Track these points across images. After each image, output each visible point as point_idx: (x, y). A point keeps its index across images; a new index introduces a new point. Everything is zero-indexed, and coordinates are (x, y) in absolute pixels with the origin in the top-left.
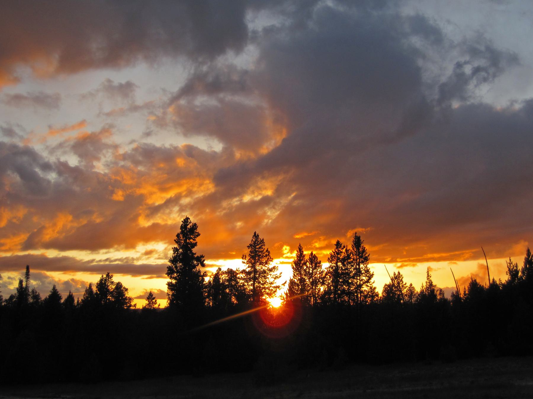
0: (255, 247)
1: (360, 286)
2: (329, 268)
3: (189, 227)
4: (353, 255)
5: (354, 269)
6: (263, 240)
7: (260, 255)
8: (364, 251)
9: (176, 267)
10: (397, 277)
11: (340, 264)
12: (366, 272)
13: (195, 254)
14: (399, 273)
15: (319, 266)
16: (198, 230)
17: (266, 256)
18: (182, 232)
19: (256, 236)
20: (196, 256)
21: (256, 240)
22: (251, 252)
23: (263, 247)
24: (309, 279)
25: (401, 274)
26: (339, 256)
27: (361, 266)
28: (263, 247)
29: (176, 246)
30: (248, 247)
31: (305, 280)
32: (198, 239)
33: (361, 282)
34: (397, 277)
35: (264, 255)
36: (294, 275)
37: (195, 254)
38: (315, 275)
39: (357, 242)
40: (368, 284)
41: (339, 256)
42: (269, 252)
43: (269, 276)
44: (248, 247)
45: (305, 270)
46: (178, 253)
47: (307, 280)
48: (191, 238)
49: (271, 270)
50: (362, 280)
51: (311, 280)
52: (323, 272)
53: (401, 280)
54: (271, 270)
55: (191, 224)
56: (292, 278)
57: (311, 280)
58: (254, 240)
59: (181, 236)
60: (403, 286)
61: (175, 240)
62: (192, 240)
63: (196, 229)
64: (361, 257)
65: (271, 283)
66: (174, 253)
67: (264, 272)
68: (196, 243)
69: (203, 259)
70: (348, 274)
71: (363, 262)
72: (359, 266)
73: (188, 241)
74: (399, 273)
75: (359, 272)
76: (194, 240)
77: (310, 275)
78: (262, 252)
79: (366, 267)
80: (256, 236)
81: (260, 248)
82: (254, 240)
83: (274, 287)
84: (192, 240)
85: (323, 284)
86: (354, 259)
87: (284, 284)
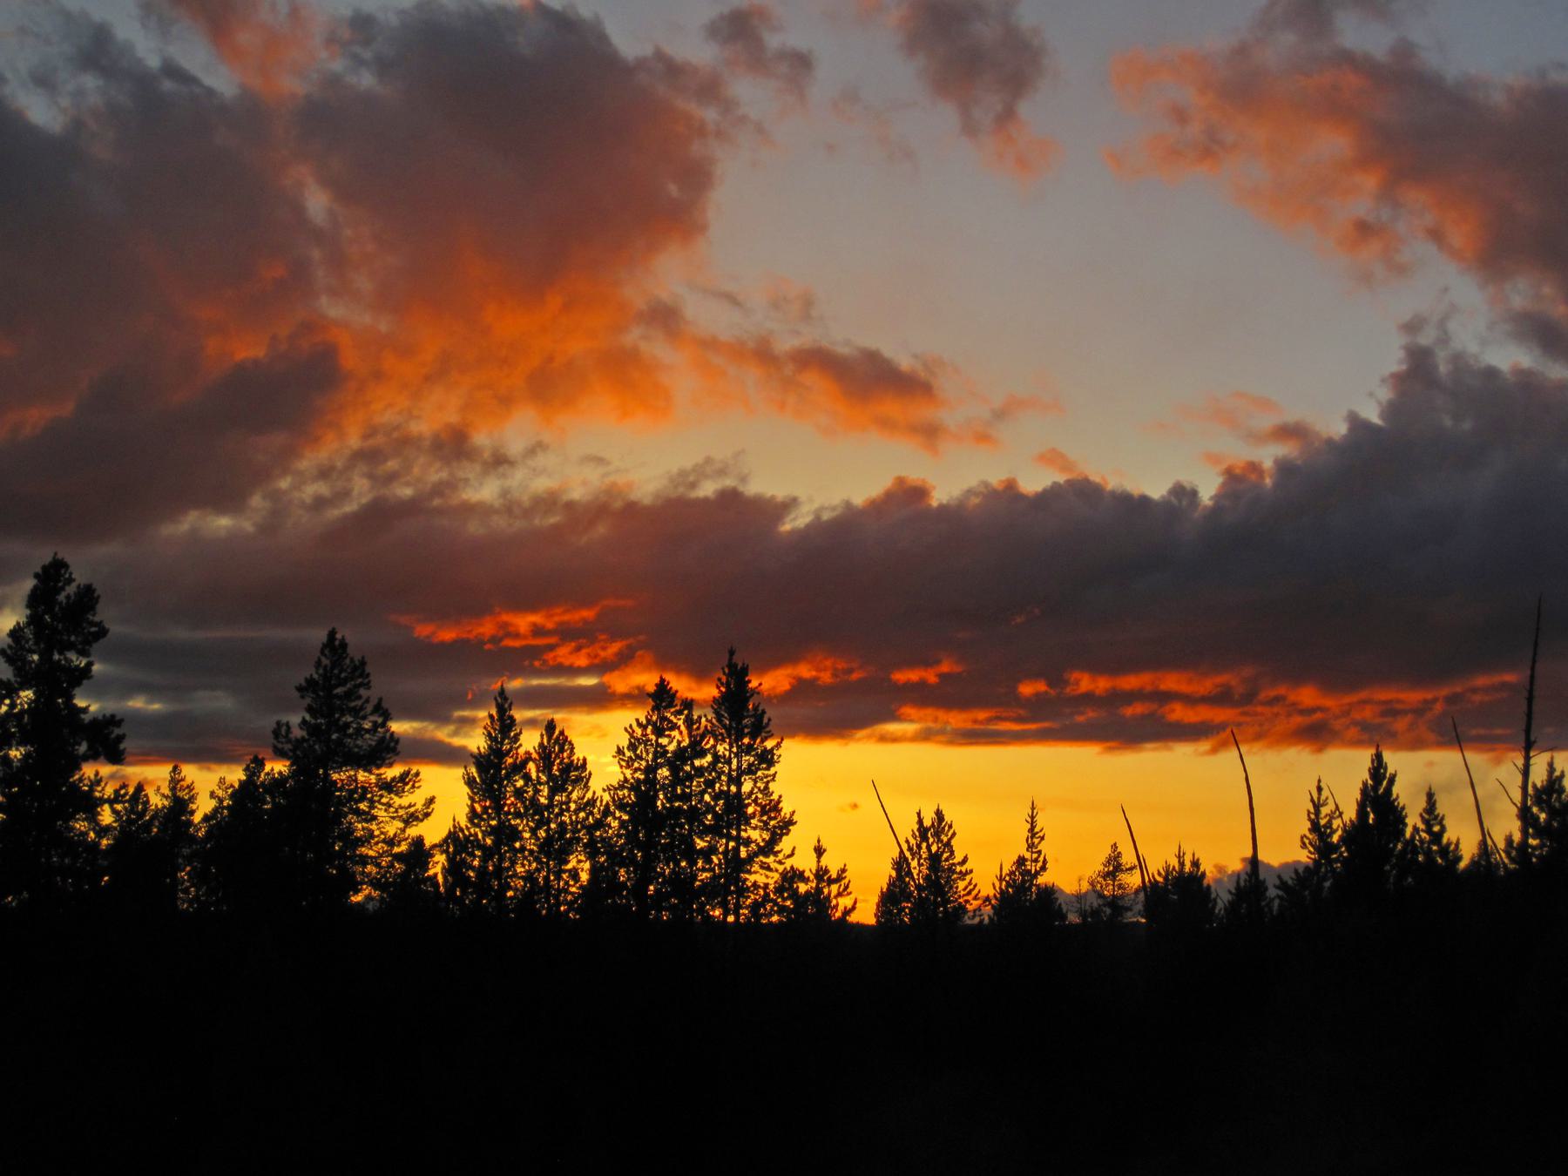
1: (737, 866)
2: (621, 787)
3: (62, 597)
5: (716, 797)
6: (363, 663)
7: (347, 725)
10: (934, 831)
11: (664, 772)
12: (764, 812)
14: (939, 815)
15: (579, 779)
16: (105, 614)
19: (334, 647)
21: (334, 665)
22: (309, 709)
23: (362, 691)
24: (534, 831)
25: (948, 819)
26: (663, 741)
28: (362, 691)
30: (300, 689)
31: (515, 834)
33: (743, 853)
34: (934, 831)
35: (367, 725)
36: (473, 809)
38: (561, 813)
40: (770, 860)
41: (663, 741)
43: (380, 812)
45: (519, 793)
46: (12, 706)
47: (527, 835)
48: (71, 646)
49: (389, 787)
51: (542, 833)
52: (592, 802)
53: (948, 844)
54: (389, 787)
55: (71, 589)
56: (464, 822)
57: (542, 833)
60: (951, 870)
64: (749, 749)
65: (391, 842)
69: (117, 731)
70: (694, 815)
71: (751, 770)
72: (739, 785)
73: (56, 657)
74: (939, 815)
75: (735, 809)
76: (83, 653)
79: (766, 791)
80: (334, 647)
81: (349, 695)
82: (325, 661)
84: (72, 656)
86: (716, 758)
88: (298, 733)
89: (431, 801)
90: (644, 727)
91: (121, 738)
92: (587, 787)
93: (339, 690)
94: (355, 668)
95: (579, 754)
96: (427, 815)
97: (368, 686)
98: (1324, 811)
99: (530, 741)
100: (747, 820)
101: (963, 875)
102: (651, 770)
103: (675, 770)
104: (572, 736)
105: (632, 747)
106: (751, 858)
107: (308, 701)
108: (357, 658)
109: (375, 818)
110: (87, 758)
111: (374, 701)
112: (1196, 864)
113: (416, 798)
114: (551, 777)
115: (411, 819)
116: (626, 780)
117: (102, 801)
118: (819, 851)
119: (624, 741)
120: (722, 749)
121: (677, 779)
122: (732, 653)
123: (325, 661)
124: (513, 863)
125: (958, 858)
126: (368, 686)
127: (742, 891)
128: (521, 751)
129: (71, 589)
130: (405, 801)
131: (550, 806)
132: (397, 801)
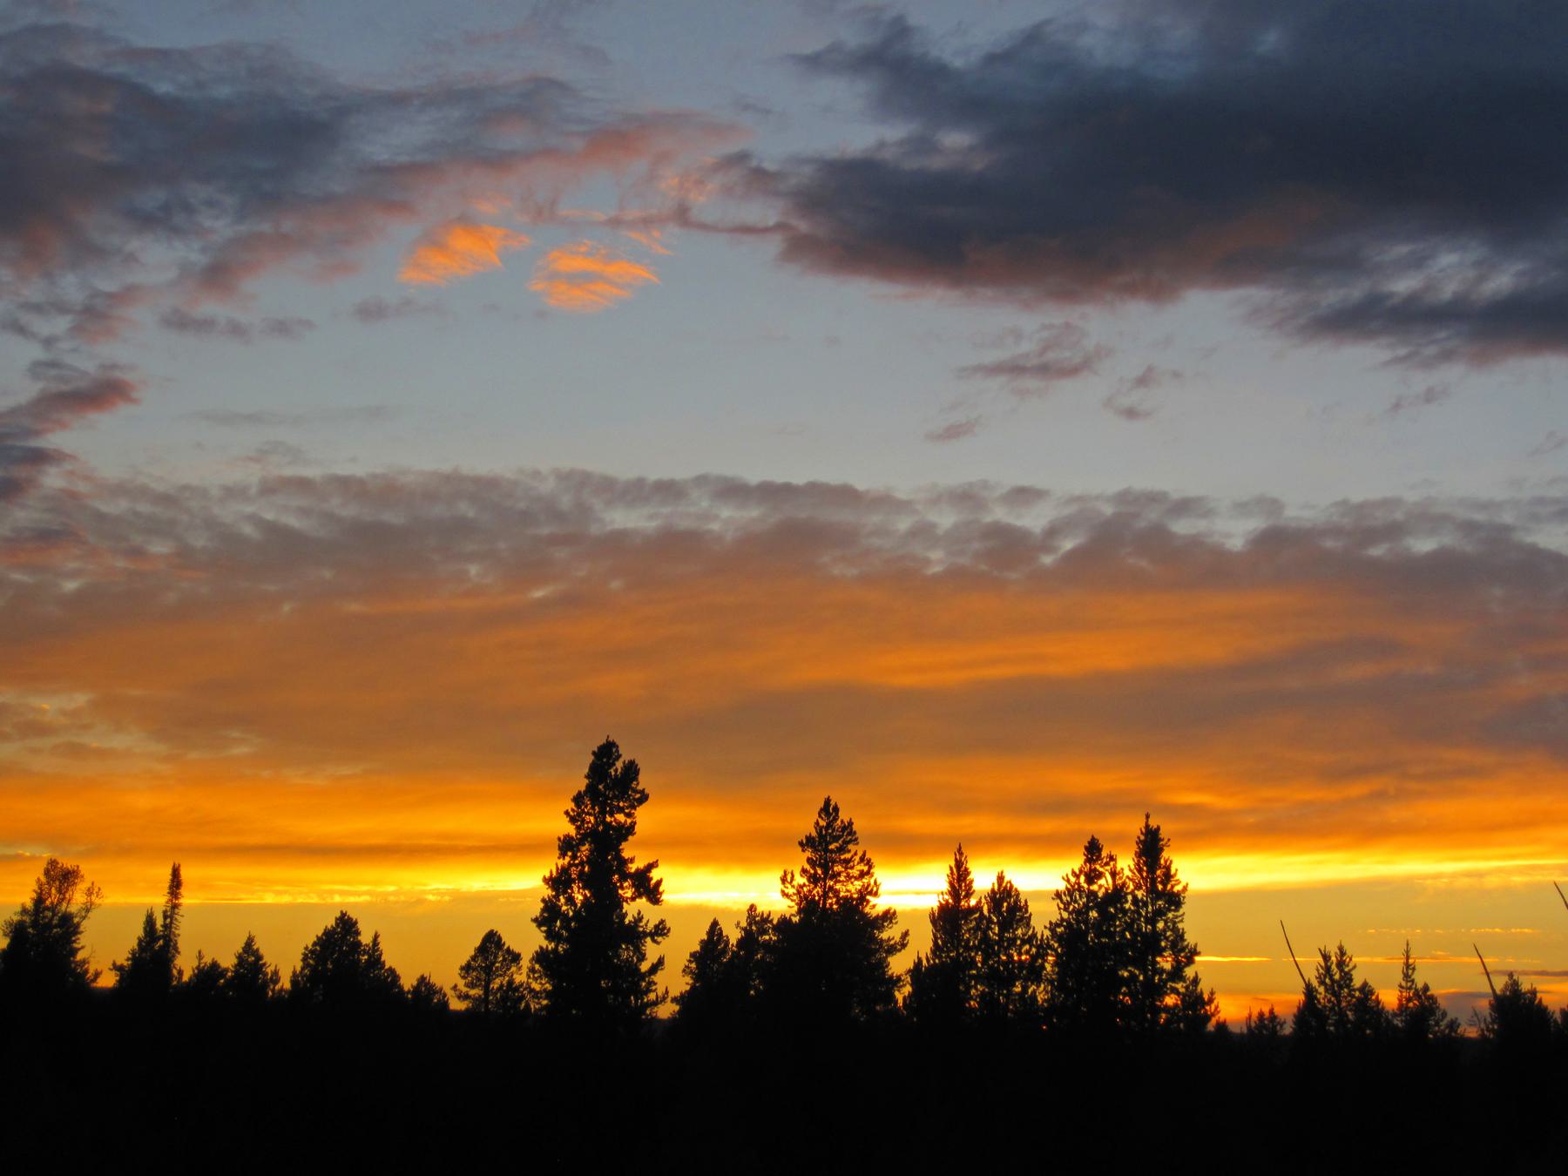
6: (851, 823)
8: (1168, 876)
11: (1094, 914)
14: (1341, 948)
16: (644, 782)
17: (862, 875)
18: (591, 790)
19: (829, 810)
20: (633, 868)
21: (829, 825)
22: (809, 860)
24: (983, 963)
26: (1095, 887)
27: (1161, 925)
28: (850, 847)
29: (571, 830)
30: (801, 844)
35: (855, 872)
36: (935, 942)
37: (632, 860)
38: (1009, 947)
39: (1151, 848)
40: (1180, 986)
41: (1095, 887)
42: (869, 864)
46: (574, 857)
48: (621, 810)
50: (1163, 971)
55: (619, 765)
58: (823, 823)
61: (567, 813)
62: (621, 817)
63: (635, 778)
66: (563, 855)
68: (633, 825)
71: (1159, 913)
72: (1154, 927)
73: (608, 819)
76: (629, 815)
77: (987, 946)
78: (847, 861)
80: (829, 810)
82: (823, 823)
84: (621, 817)
89: (906, 934)
90: (1078, 877)
91: (659, 883)
92: (1028, 925)
93: (832, 847)
94: (844, 828)
96: (904, 946)
97: (855, 841)
102: (1081, 913)
107: (808, 854)
108: (846, 821)
110: (633, 899)
111: (860, 854)
116: (1062, 920)
117: (645, 934)
121: (1105, 917)
122: (1148, 817)
124: (968, 988)
126: (855, 841)
127: (1156, 1011)
129: (619, 765)
131: (998, 943)
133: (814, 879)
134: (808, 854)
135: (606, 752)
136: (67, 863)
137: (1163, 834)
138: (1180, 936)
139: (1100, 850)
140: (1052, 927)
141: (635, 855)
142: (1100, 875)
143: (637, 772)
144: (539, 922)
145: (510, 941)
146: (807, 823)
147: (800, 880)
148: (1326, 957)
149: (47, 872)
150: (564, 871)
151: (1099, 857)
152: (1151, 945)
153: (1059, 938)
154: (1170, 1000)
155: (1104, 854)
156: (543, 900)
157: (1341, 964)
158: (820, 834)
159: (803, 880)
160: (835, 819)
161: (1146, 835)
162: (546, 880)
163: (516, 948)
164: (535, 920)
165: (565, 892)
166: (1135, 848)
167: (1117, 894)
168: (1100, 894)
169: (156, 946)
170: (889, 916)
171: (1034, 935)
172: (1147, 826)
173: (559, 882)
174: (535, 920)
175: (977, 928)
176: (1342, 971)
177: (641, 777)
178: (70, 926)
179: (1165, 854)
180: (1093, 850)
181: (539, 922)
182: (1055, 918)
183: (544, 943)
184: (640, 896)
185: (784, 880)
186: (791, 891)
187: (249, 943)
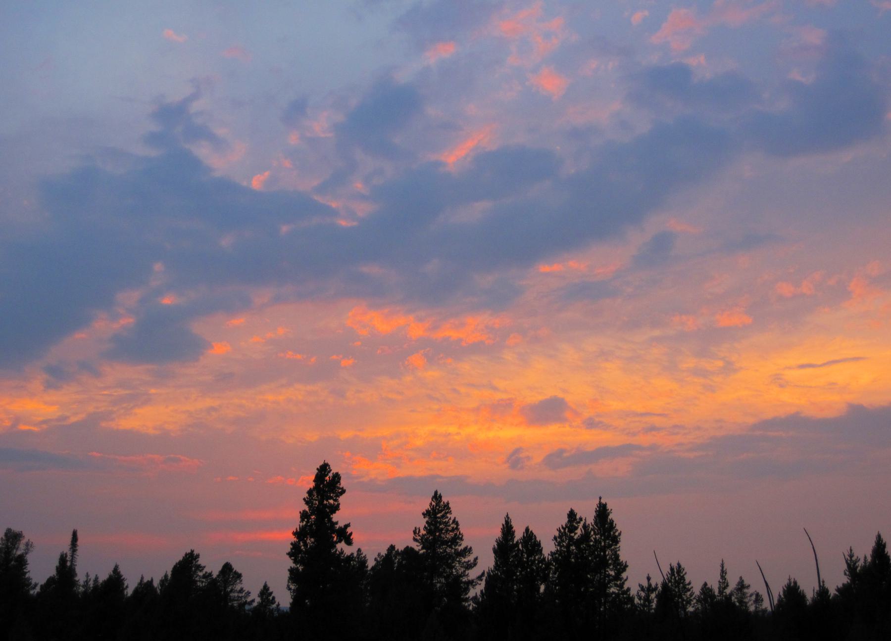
0: (435, 513)
1: (605, 586)
3: (327, 478)
4: (595, 534)
6: (448, 503)
7: (442, 529)
9: (305, 544)
13: (337, 523)
16: (343, 483)
18: (317, 488)
19: (437, 497)
20: (337, 526)
22: (427, 522)
23: (448, 515)
28: (448, 515)
29: (306, 508)
30: (423, 514)
32: (342, 499)
35: (450, 528)
36: (496, 563)
37: (337, 523)
38: (532, 565)
42: (457, 524)
44: (423, 514)
46: (307, 522)
48: (331, 498)
50: (609, 575)
55: (331, 475)
59: (315, 493)
60: (684, 587)
61: (304, 499)
62: (331, 501)
63: (339, 481)
66: (302, 520)
67: (450, 556)
68: (339, 504)
71: (610, 546)
72: (605, 553)
76: (335, 500)
80: (437, 497)
81: (443, 516)
82: (433, 503)
83: (465, 583)
84: (331, 501)
85: (545, 579)
87: (480, 578)
88: (423, 532)
89: (476, 559)
90: (564, 529)
91: (351, 534)
92: (541, 554)
93: (439, 515)
94: (445, 506)
95: (538, 539)
98: (854, 559)
99: (519, 535)
100: (608, 565)
101: (689, 590)
102: (568, 546)
103: (578, 547)
104: (535, 533)
105: (560, 537)
106: (610, 582)
107: (427, 519)
109: (453, 567)
112: (795, 583)
113: (470, 558)
114: (527, 549)
115: (470, 566)
118: (649, 579)
119: (557, 534)
120: (598, 537)
122: (600, 498)
123: (433, 503)
125: (687, 582)
126: (450, 512)
128: (515, 540)
129: (331, 475)
130: (466, 560)
132: (463, 560)
133: (429, 532)
134: (427, 519)
135: (324, 469)
136: (16, 529)
137: (609, 507)
138: (617, 557)
139: (575, 516)
140: (552, 554)
141: (339, 518)
142: (576, 528)
143: (339, 478)
144: (290, 555)
145: (236, 567)
146: (426, 504)
147: (423, 532)
148: (672, 569)
149: (6, 535)
150: (303, 529)
151: (575, 519)
152: (603, 563)
153: (556, 560)
154: (612, 590)
155: (578, 517)
156: (292, 544)
157: (679, 572)
158: (433, 509)
159: (424, 532)
160: (440, 501)
161: (599, 507)
162: (294, 534)
163: (239, 571)
164: (288, 554)
165: (303, 540)
166: (594, 514)
167: (586, 537)
168: (576, 537)
169: (65, 570)
170: (467, 551)
171: (544, 559)
172: (600, 503)
173: (300, 534)
174: (288, 554)
175: (516, 555)
176: (679, 575)
177: (342, 481)
178: (21, 561)
179: (610, 517)
180: (572, 515)
181: (290, 555)
182: (554, 549)
183: (293, 565)
184: (340, 541)
185: (415, 532)
186: (418, 538)
187: (116, 570)
